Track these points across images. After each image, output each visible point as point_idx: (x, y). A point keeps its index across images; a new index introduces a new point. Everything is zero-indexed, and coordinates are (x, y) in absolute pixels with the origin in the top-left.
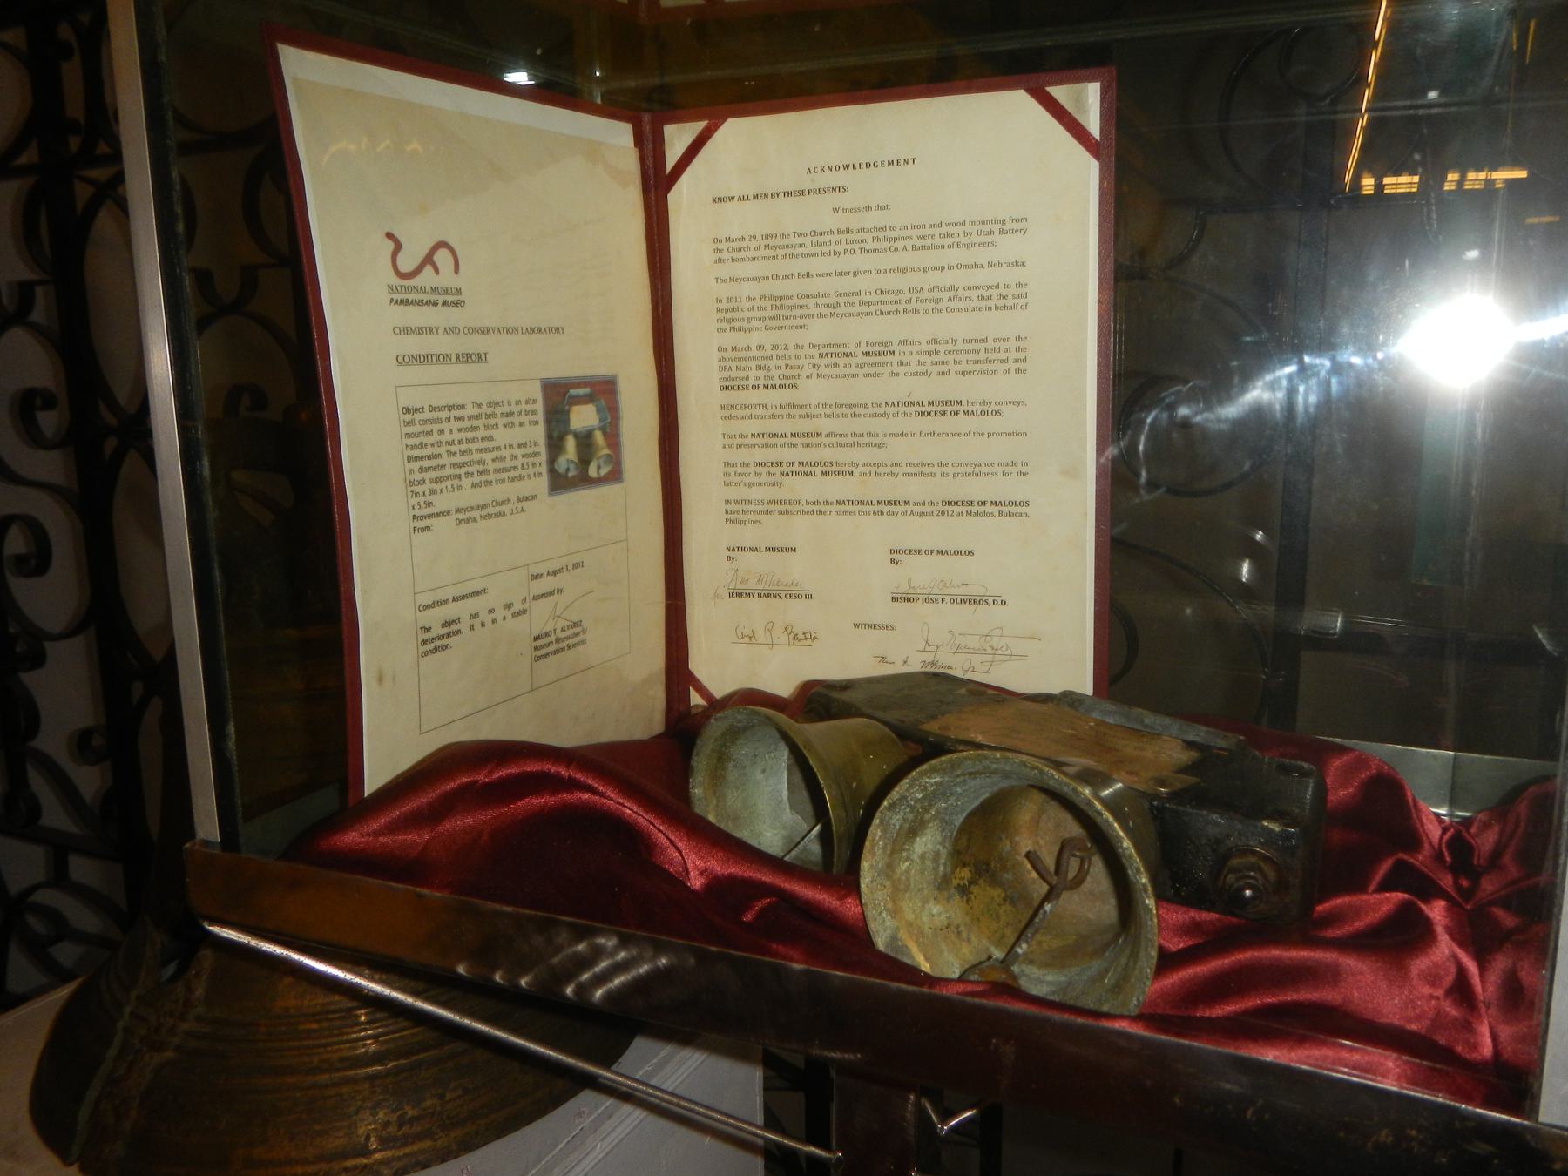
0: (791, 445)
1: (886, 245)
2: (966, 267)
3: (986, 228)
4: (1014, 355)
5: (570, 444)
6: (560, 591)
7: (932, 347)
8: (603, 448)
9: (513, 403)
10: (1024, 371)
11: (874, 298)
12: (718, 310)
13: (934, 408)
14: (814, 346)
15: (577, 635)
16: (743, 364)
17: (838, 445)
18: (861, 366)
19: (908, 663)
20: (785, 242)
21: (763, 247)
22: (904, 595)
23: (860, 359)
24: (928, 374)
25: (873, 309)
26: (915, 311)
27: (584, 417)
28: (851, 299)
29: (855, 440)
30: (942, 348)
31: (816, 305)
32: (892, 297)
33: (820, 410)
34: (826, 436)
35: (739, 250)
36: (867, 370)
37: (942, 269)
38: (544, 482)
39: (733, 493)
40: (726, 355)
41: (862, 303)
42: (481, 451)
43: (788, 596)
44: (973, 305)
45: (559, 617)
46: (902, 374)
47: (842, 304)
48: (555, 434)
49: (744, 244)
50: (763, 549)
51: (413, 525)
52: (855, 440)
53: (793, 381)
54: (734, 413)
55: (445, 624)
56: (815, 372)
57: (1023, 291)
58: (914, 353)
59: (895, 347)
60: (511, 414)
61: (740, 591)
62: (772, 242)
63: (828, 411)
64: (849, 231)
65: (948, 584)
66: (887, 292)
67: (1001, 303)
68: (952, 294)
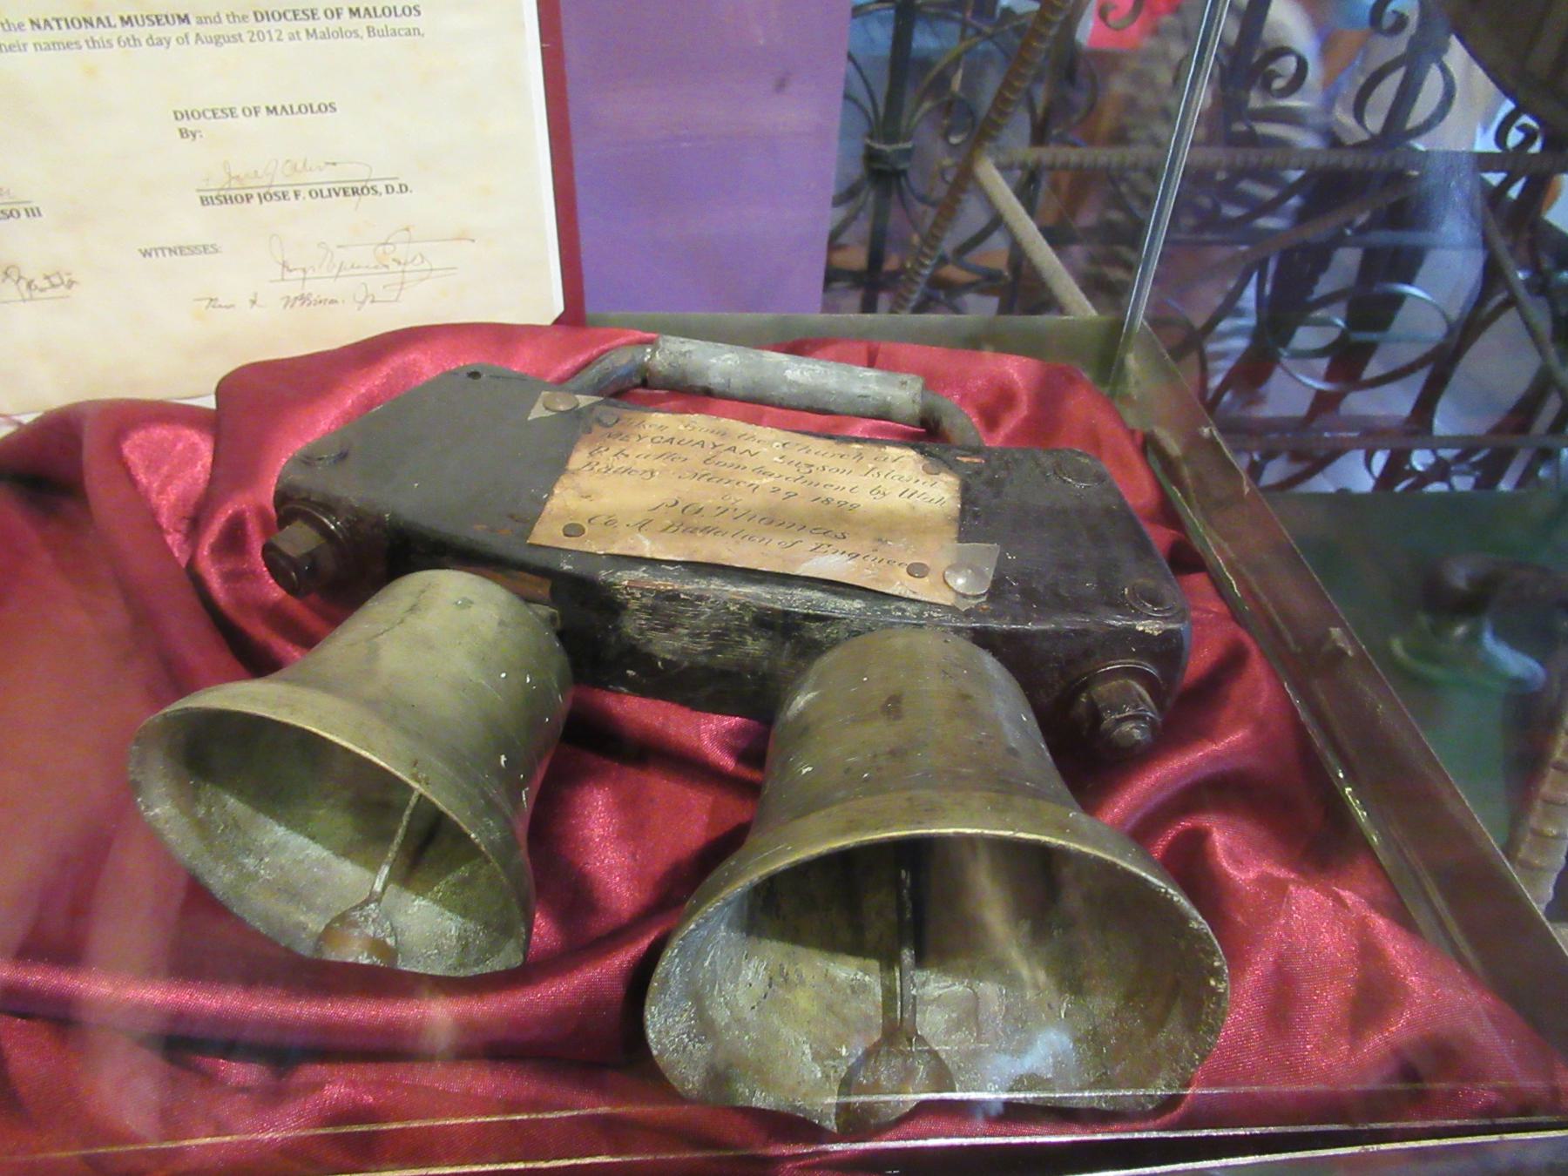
22: (222, 193)
65: (300, 166)
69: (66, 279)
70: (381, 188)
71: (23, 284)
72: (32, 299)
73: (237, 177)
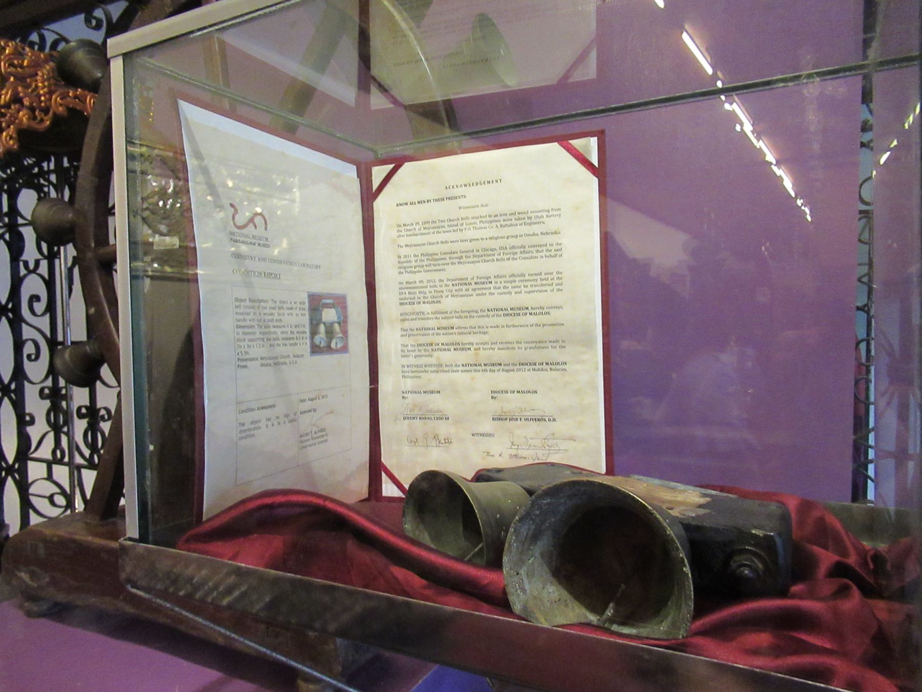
0: (437, 334)
1: (487, 225)
2: (529, 235)
3: (539, 214)
4: (556, 281)
5: (322, 328)
6: (315, 410)
7: (512, 279)
8: (338, 333)
9: (293, 303)
10: (561, 290)
11: (481, 253)
12: (399, 262)
13: (514, 312)
14: (450, 280)
15: (323, 436)
16: (412, 291)
17: (462, 333)
18: (474, 290)
19: (502, 456)
20: (434, 225)
21: (422, 228)
23: (474, 286)
24: (510, 293)
25: (480, 259)
26: (502, 260)
27: (329, 315)
28: (468, 254)
29: (472, 331)
30: (517, 279)
31: (450, 258)
32: (491, 252)
33: (453, 314)
34: (456, 328)
35: (410, 230)
36: (477, 292)
37: (516, 236)
38: (308, 348)
39: (405, 361)
40: (403, 286)
41: (474, 256)
42: (274, 327)
43: (436, 418)
44: (533, 255)
45: (314, 425)
46: (496, 294)
47: (464, 257)
48: (314, 322)
49: (412, 227)
50: (422, 392)
51: (237, 363)
52: (472, 331)
53: (438, 299)
54: (407, 317)
55: (252, 423)
56: (450, 294)
57: (559, 247)
58: (503, 282)
59: (492, 279)
60: (292, 308)
61: (409, 416)
62: (427, 225)
63: (457, 315)
64: (467, 218)
66: (487, 250)
67: (548, 254)
68: (522, 250)
69: (449, 441)
70: (547, 419)
71: (438, 441)
72: (439, 446)
73: (504, 412)
